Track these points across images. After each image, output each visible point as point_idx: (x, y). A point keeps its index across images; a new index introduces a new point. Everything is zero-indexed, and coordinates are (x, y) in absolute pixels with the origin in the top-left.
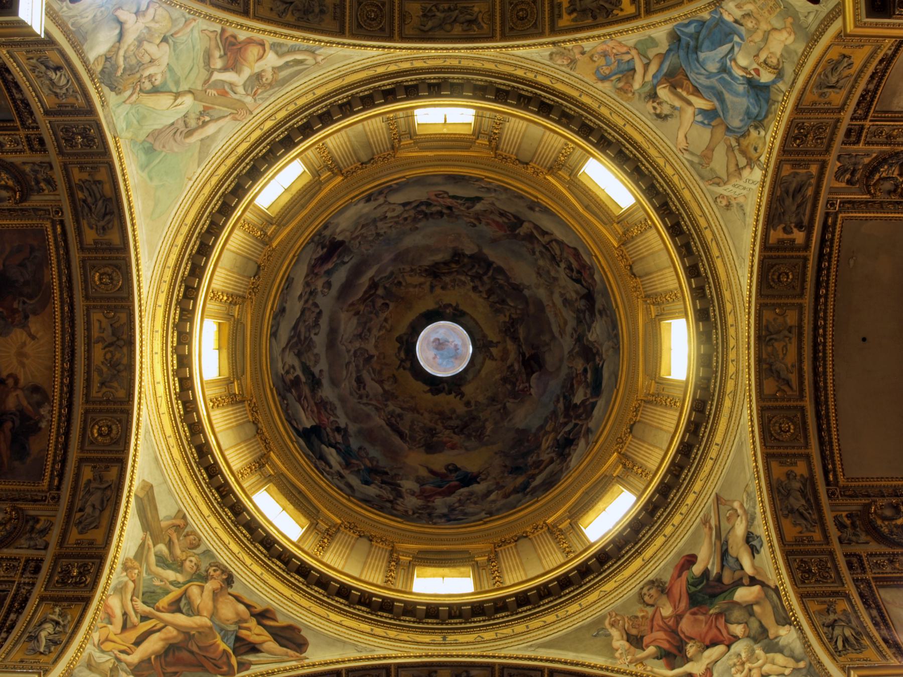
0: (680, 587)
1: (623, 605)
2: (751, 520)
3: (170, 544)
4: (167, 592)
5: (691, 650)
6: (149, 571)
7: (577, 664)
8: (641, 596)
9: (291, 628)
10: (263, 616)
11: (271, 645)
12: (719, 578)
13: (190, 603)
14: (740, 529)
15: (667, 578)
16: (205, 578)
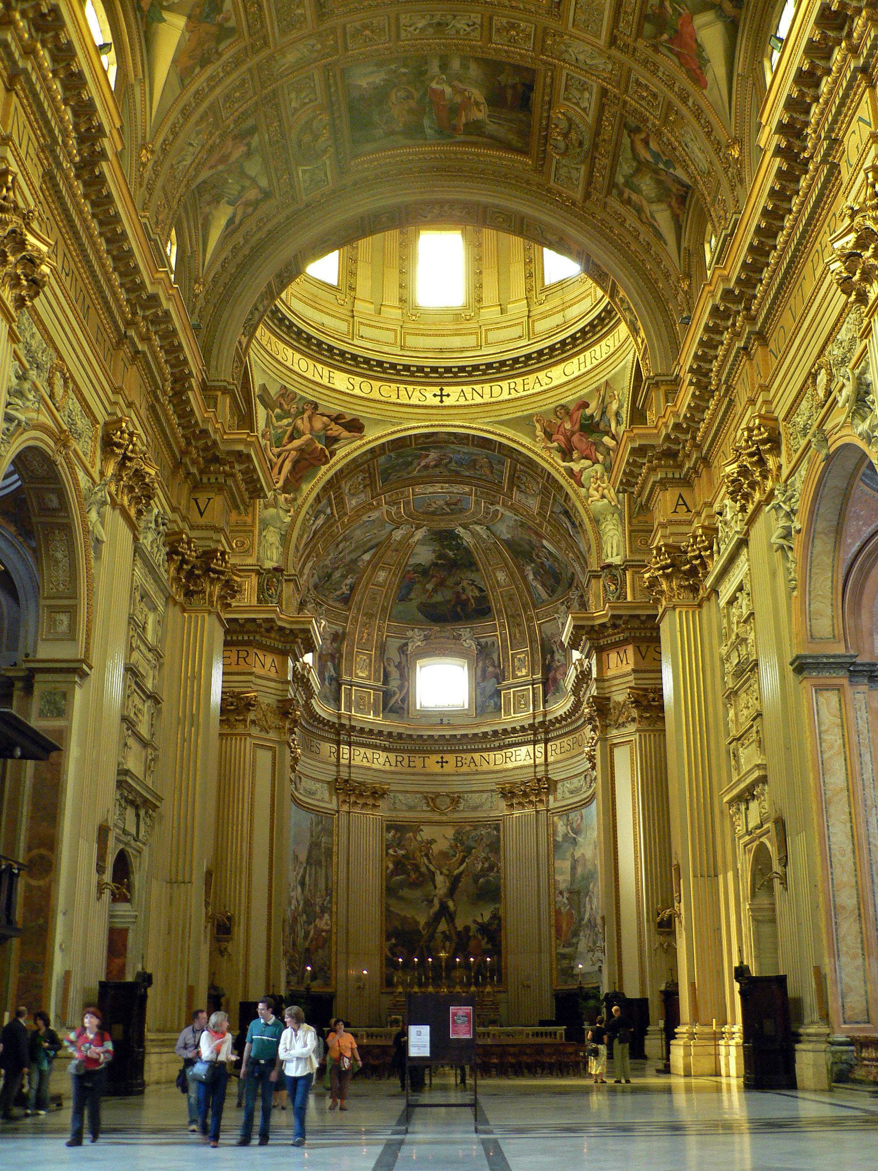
0: (577, 416)
1: (545, 412)
2: (621, 406)
3: (281, 406)
4: (285, 432)
5: (575, 455)
6: (275, 428)
7: (515, 441)
8: (556, 412)
9: (353, 420)
10: (337, 419)
11: (345, 434)
12: (598, 424)
13: (298, 431)
14: (614, 406)
15: (572, 407)
16: (303, 413)
